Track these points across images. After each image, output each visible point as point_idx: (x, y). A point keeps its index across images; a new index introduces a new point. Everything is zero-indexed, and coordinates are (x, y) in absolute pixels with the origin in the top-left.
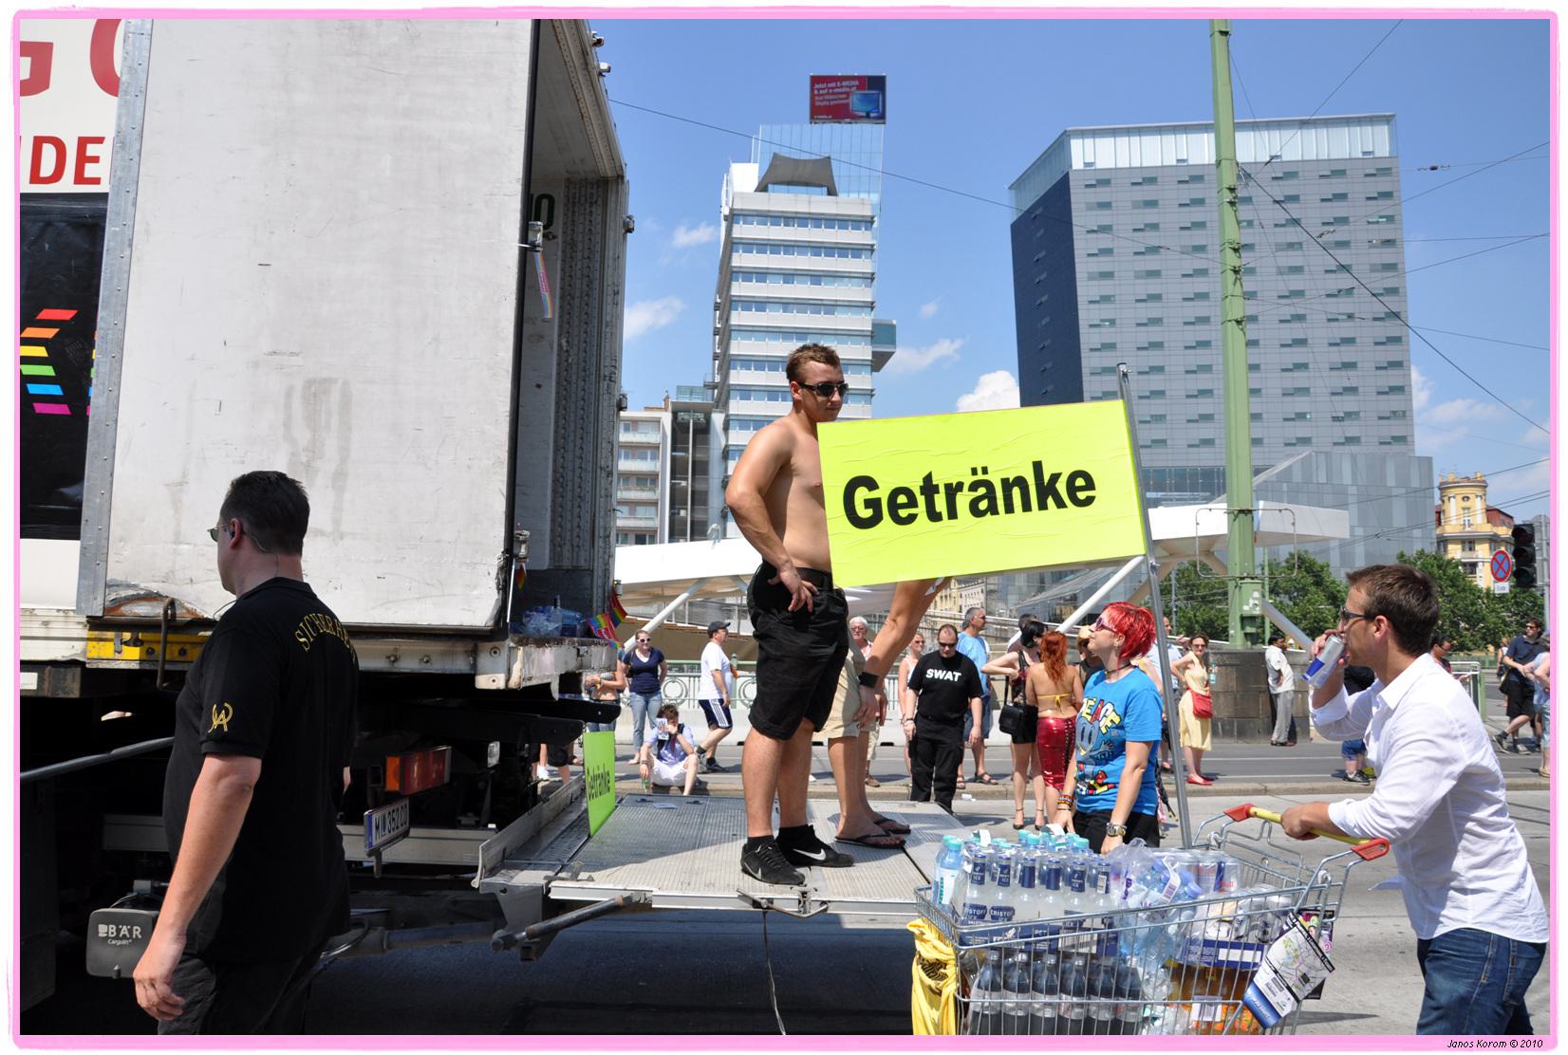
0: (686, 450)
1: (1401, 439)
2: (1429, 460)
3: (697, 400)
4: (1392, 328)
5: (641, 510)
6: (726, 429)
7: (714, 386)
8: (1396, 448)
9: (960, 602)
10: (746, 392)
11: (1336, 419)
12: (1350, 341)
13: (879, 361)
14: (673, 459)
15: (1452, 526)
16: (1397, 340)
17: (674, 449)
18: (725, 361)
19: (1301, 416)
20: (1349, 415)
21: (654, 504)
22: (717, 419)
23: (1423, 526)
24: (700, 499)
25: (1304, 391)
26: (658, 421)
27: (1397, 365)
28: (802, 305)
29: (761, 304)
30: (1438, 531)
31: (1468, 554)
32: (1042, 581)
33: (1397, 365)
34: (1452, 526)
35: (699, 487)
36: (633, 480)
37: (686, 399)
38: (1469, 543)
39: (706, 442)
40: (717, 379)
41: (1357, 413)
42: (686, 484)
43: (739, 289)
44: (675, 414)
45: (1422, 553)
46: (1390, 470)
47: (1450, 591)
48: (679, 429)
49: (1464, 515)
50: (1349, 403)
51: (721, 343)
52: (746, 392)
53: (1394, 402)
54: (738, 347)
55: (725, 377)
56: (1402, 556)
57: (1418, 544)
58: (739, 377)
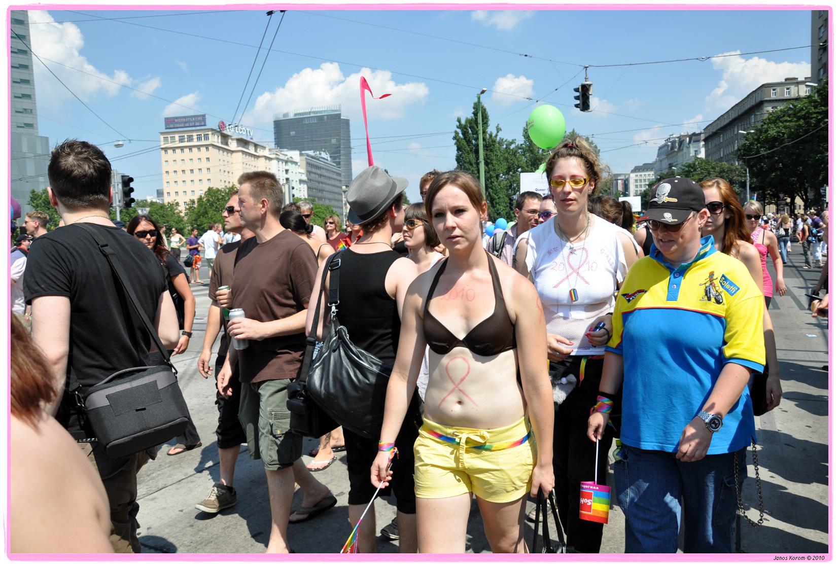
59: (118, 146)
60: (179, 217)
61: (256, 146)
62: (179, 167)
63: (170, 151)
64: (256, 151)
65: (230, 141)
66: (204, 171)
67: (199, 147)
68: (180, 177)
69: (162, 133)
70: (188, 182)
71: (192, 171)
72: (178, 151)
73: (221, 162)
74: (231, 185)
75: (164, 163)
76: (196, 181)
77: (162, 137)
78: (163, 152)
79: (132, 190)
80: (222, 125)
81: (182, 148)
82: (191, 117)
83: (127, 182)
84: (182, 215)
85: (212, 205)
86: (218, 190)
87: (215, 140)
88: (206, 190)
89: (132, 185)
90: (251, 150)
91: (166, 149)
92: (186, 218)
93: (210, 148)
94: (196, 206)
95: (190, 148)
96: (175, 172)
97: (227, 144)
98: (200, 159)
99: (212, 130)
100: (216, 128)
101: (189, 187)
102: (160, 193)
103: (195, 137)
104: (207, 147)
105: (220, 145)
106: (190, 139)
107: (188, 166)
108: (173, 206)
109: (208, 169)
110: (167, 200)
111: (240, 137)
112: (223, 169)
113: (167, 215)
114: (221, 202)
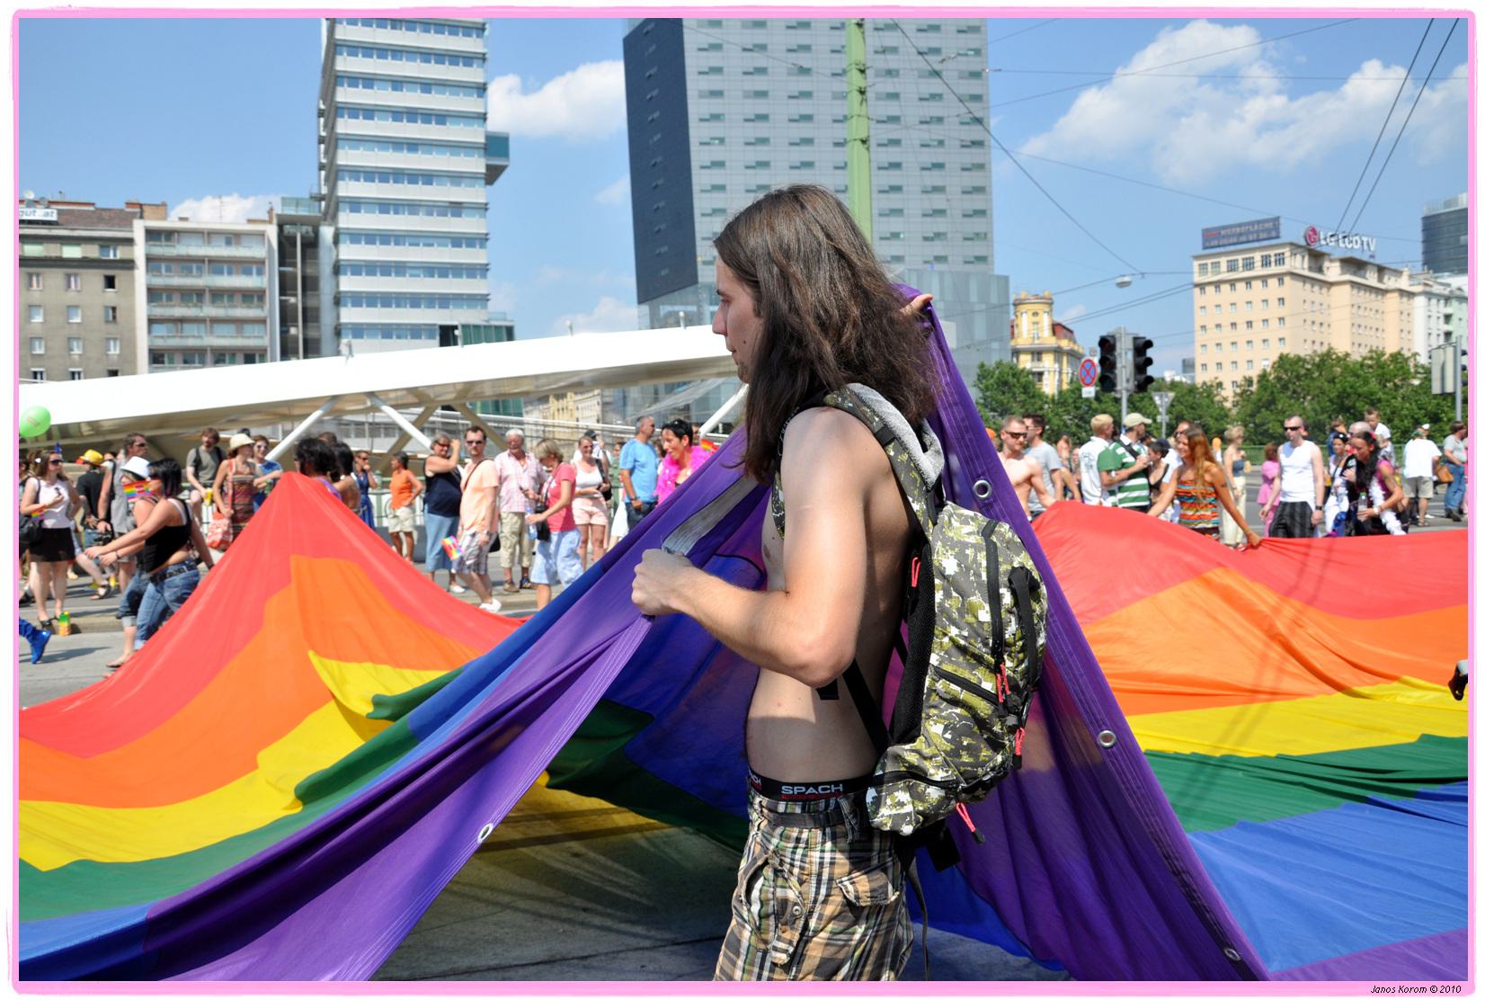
0: (294, 265)
1: (982, 259)
2: (1006, 279)
3: (303, 212)
4: (974, 156)
5: (248, 328)
6: (336, 241)
7: (321, 198)
8: (980, 267)
9: (576, 414)
10: (356, 204)
11: (926, 239)
12: (939, 166)
13: (492, 174)
14: (282, 275)
15: (1024, 338)
16: (981, 167)
17: (281, 264)
18: (333, 173)
19: (895, 235)
20: (938, 235)
21: (263, 321)
22: (327, 232)
23: (1001, 340)
24: (311, 316)
25: (897, 212)
26: (262, 235)
27: (979, 190)
28: (412, 115)
29: (369, 112)
30: (1012, 343)
31: (1036, 364)
32: (656, 392)
33: (979, 190)
34: (1024, 338)
35: (311, 303)
36: (238, 297)
37: (291, 211)
38: (1037, 354)
39: (316, 257)
40: (324, 190)
41: (944, 234)
42: (296, 300)
43: (344, 95)
44: (281, 227)
45: (999, 364)
46: (974, 287)
47: (1023, 397)
48: (286, 244)
49: (1032, 328)
50: (940, 225)
51: (326, 153)
52: (356, 204)
53: (977, 225)
54: (346, 157)
55: (333, 188)
56: (982, 366)
57: (995, 357)
58: (347, 188)
59: (1122, 285)
60: (1222, 408)
61: (1381, 270)
62: (1226, 317)
63: (1210, 289)
64: (1380, 280)
65: (1326, 264)
66: (1274, 323)
67: (1264, 279)
68: (1227, 335)
69: (1197, 258)
70: (1242, 345)
71: (1249, 324)
72: (1225, 288)
73: (1307, 306)
74: (1325, 349)
75: (1198, 312)
76: (1258, 343)
77: (1196, 263)
78: (1197, 290)
79: (1149, 362)
80: (1312, 234)
81: (1232, 283)
82: (1252, 223)
83: (1142, 347)
84: (1228, 405)
85: (1285, 387)
86: (1299, 359)
87: (1299, 264)
88: (1275, 358)
89: (1150, 353)
90: (1371, 279)
91: (1202, 286)
92: (1234, 411)
93: (1287, 279)
94: (1254, 388)
95: (1248, 281)
96: (1218, 326)
97: (1320, 270)
98: (1265, 301)
99: (1292, 244)
100: (1303, 243)
101: (1242, 353)
102: (1188, 366)
103: (1258, 264)
104: (1280, 277)
105: (1306, 273)
106: (1249, 265)
107: (1241, 316)
108: (1210, 390)
109: (1281, 319)
110: (1201, 377)
111: (1349, 255)
112: (1310, 318)
113: (1199, 406)
114: (1305, 382)
